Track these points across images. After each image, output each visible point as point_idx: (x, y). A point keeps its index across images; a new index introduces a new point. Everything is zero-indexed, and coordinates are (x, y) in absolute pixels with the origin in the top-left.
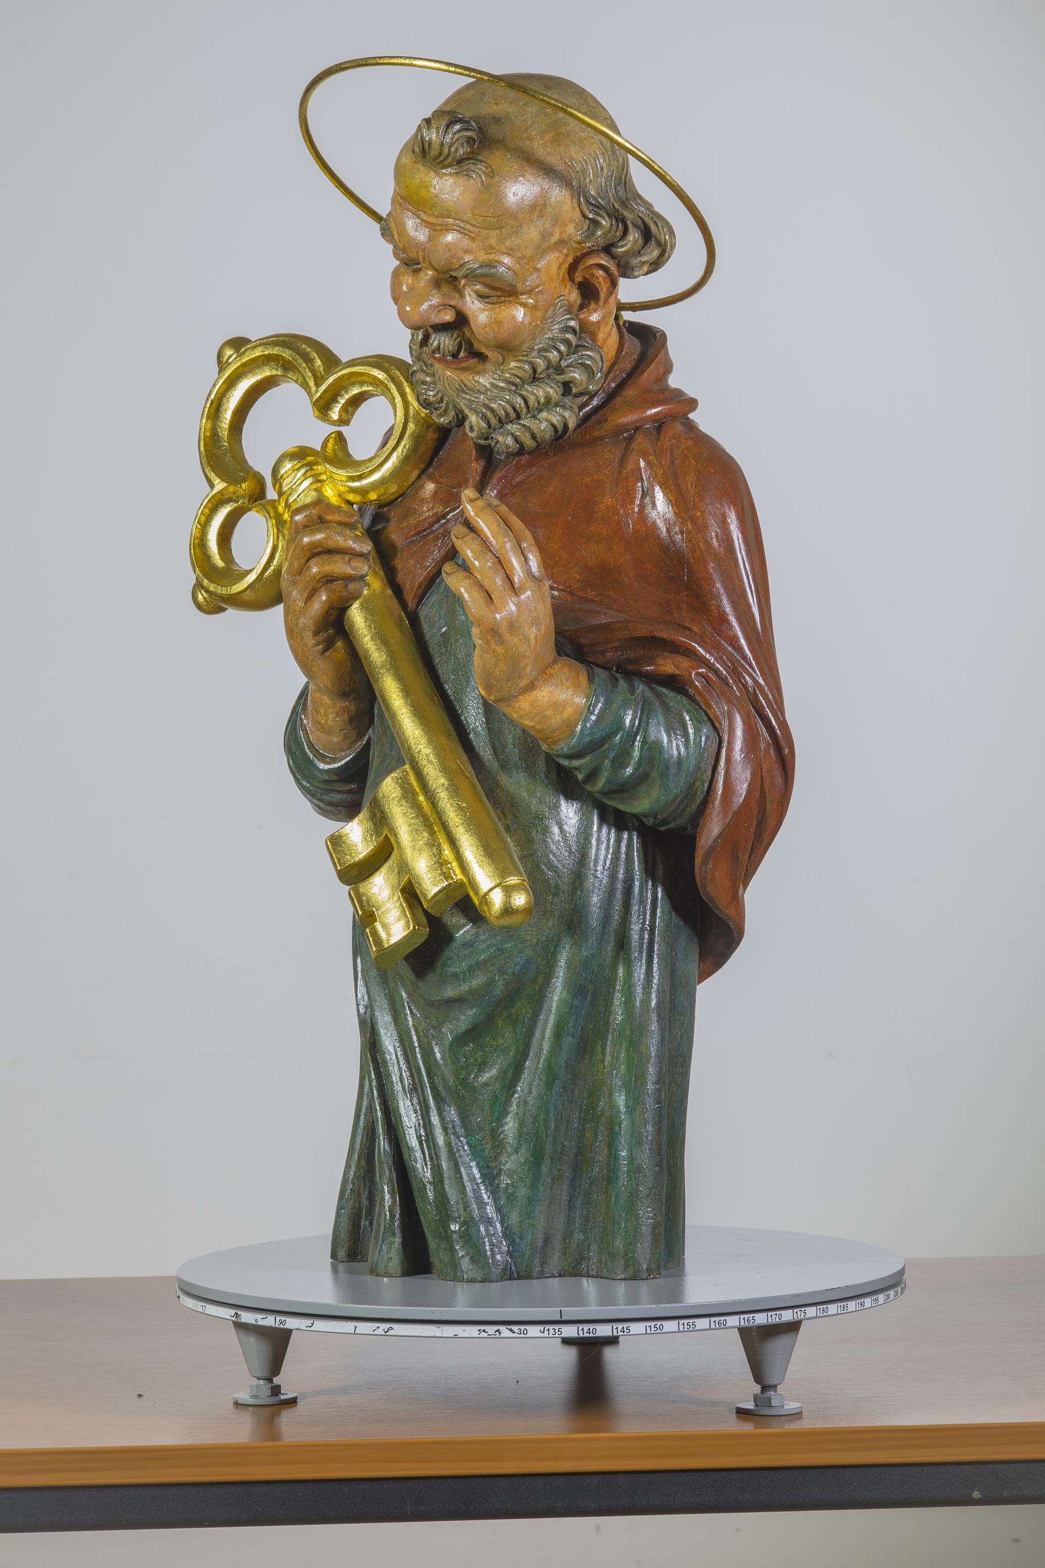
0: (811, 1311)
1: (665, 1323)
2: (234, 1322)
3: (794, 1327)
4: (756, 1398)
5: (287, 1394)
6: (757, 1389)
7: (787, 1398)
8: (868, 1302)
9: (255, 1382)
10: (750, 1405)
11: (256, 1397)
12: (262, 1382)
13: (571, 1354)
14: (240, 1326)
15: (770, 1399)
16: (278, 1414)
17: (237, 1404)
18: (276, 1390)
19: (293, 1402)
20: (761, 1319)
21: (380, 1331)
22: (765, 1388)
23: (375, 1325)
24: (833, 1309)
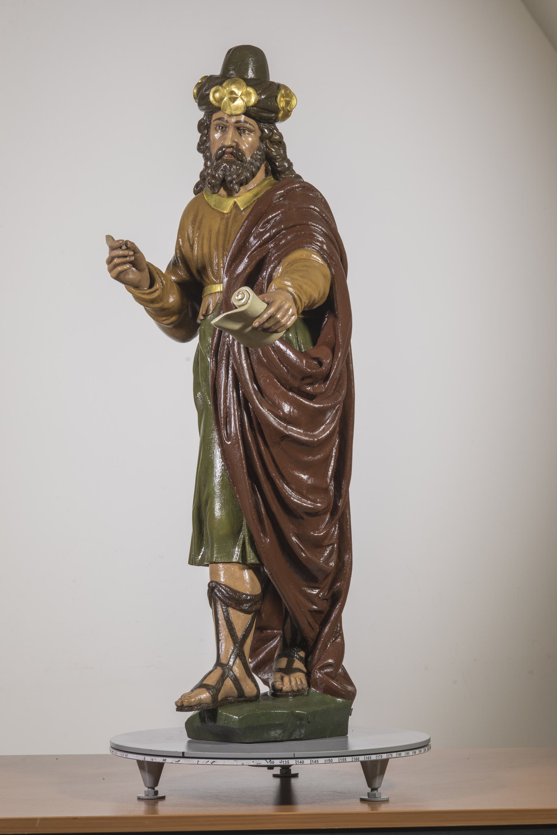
0: (394, 755)
1: (333, 759)
2: (139, 762)
3: (385, 762)
4: (368, 794)
5: (160, 794)
6: (369, 790)
7: (383, 792)
8: (417, 751)
9: (147, 789)
10: (367, 797)
11: (147, 795)
12: (150, 789)
13: (277, 781)
14: (141, 764)
15: (375, 794)
16: (157, 803)
17: (139, 799)
18: (156, 793)
19: (163, 798)
20: (374, 757)
21: (209, 763)
22: (373, 790)
23: (208, 760)
24: (403, 754)
